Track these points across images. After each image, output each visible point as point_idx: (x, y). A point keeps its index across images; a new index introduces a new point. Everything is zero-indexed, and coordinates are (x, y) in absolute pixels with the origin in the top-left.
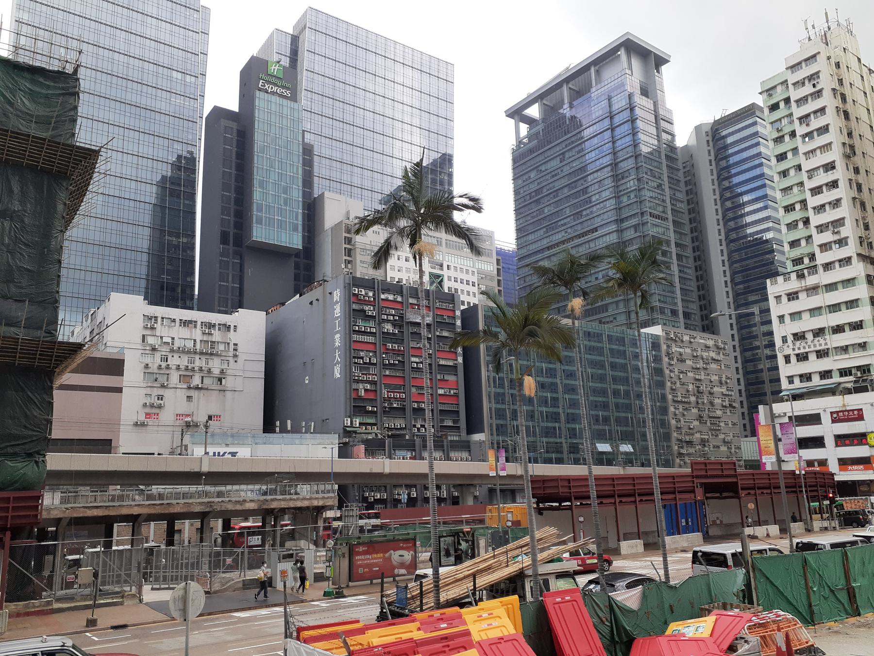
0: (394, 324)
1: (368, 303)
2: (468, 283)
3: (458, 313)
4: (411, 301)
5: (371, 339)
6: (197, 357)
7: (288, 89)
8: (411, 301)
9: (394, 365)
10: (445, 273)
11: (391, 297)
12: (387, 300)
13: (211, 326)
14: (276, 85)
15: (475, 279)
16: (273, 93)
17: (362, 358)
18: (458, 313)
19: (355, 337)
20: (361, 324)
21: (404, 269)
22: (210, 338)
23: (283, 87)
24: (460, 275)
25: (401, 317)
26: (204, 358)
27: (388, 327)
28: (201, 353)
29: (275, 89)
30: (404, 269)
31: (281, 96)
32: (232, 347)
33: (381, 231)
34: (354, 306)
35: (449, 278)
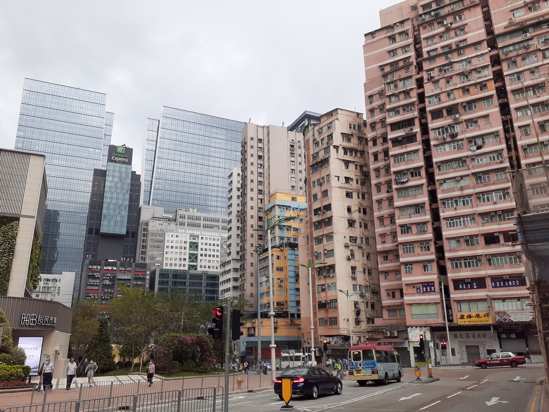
0: (110, 280)
1: (98, 272)
2: (214, 245)
3: (148, 273)
4: (121, 269)
5: (97, 288)
6: (40, 294)
7: (127, 158)
8: (121, 269)
9: (107, 299)
10: (200, 241)
11: (110, 268)
12: (108, 270)
13: (48, 280)
14: (120, 157)
15: (219, 243)
16: (118, 162)
17: (90, 297)
18: (148, 273)
19: (88, 287)
20: (91, 281)
21: (175, 242)
22: (47, 286)
23: (124, 158)
24: (209, 242)
25: (114, 277)
26: (43, 294)
27: (107, 282)
28: (43, 292)
29: (120, 159)
30: (175, 242)
31: (123, 163)
32: (57, 288)
33: (164, 224)
34: (90, 274)
35: (202, 244)
